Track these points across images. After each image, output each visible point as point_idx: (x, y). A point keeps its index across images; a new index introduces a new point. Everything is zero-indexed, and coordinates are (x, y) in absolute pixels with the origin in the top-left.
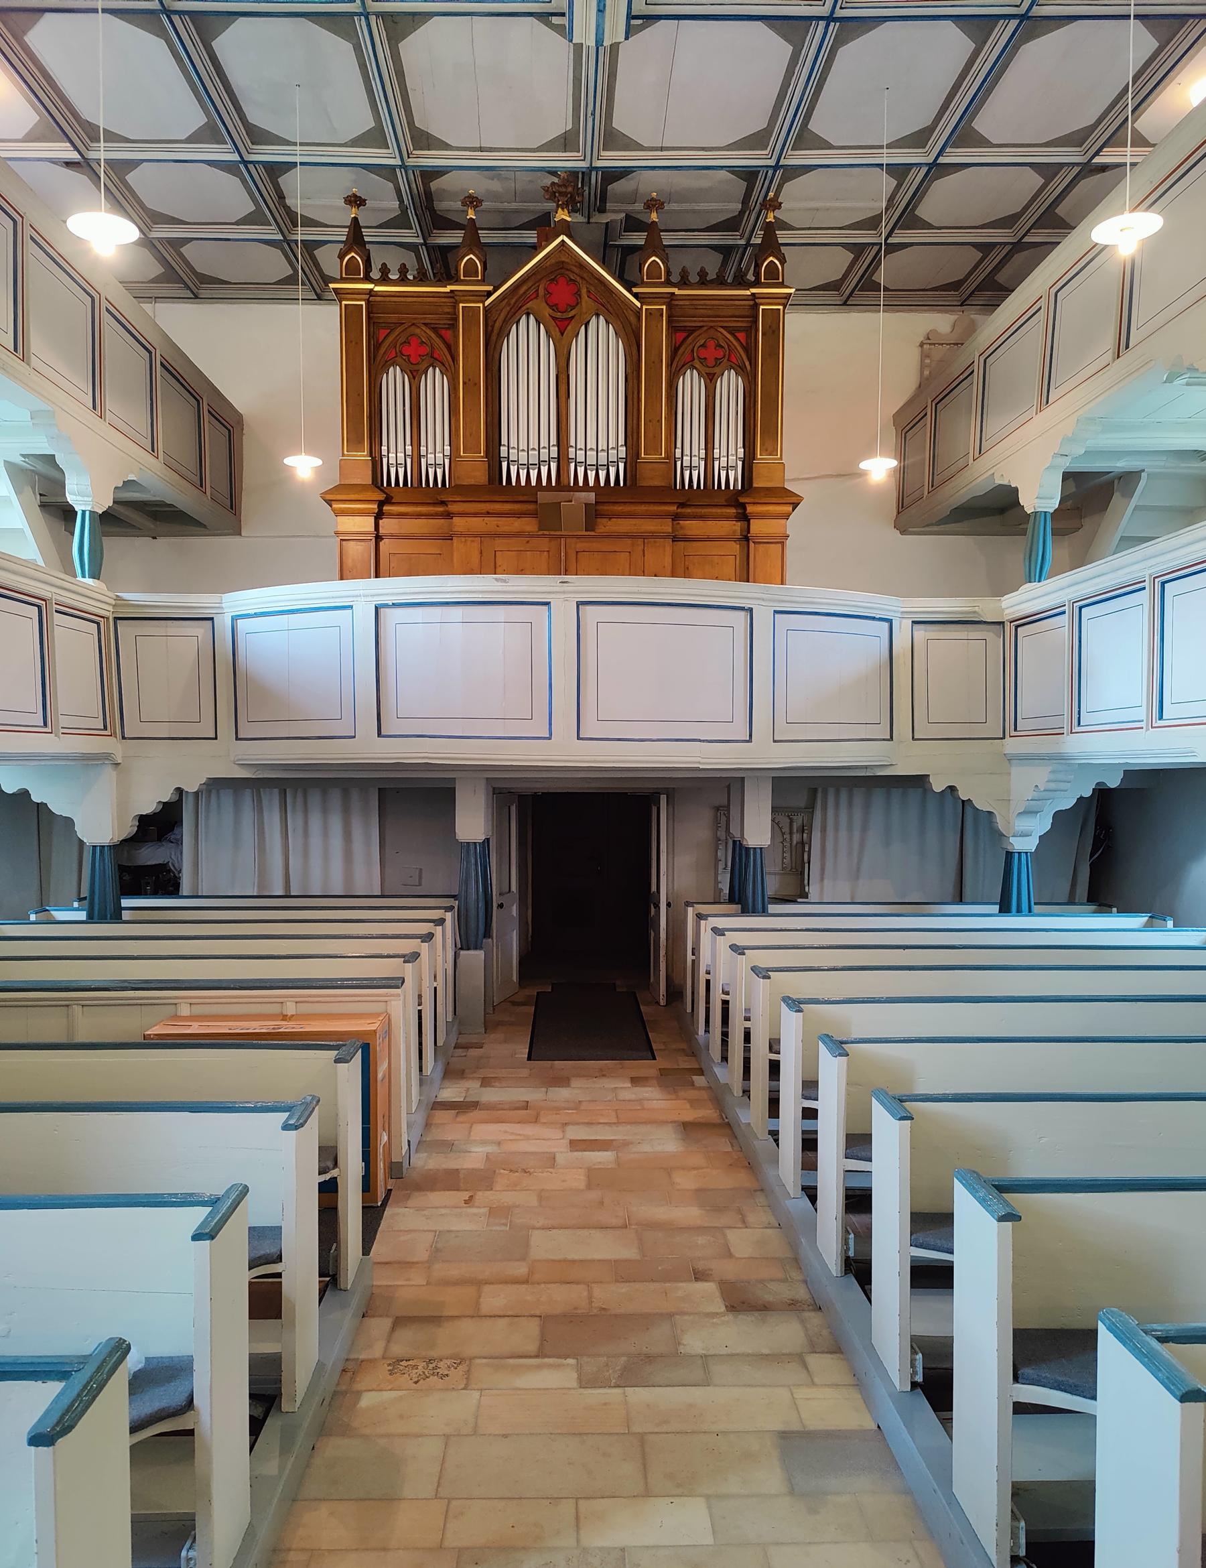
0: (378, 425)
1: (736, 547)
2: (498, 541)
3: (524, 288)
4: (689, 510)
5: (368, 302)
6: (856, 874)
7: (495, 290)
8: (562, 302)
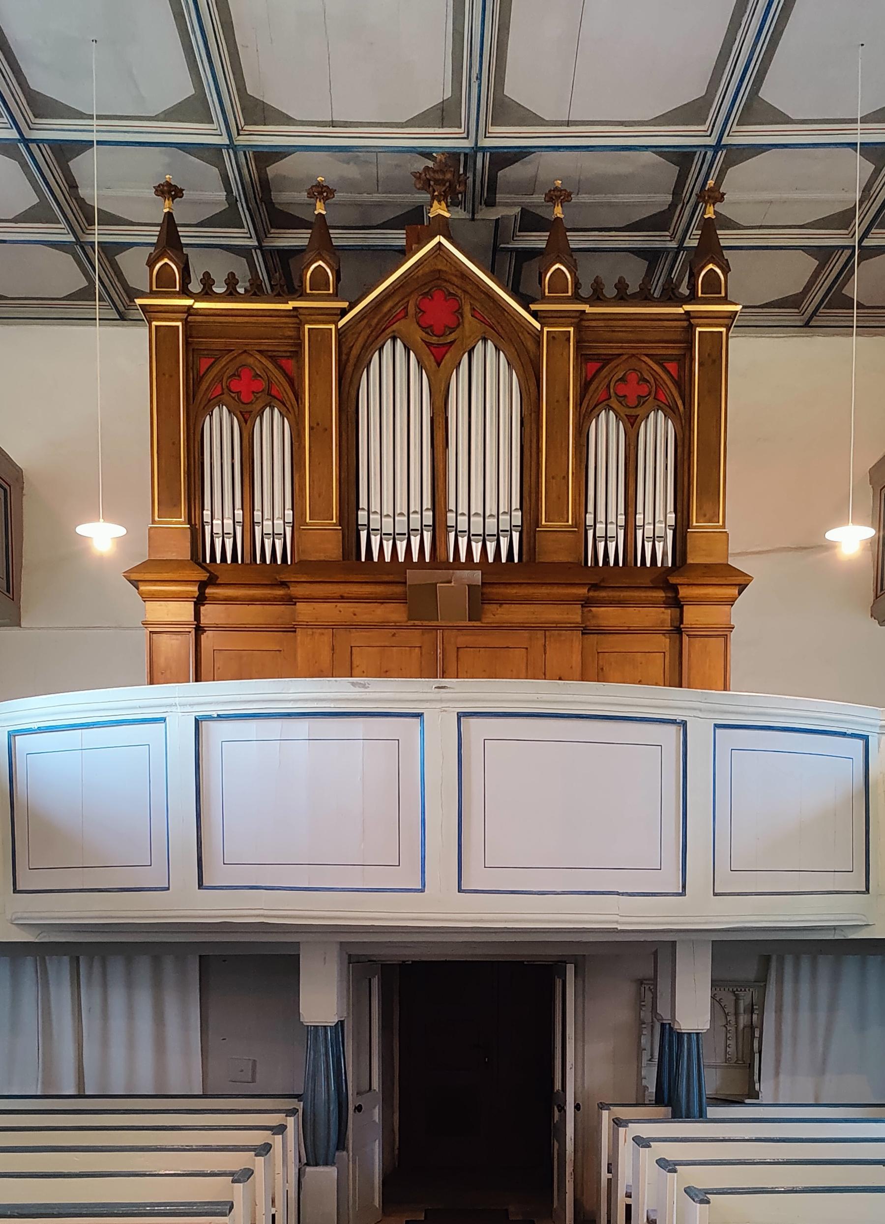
0: (198, 482)
4: (603, 594)
7: (352, 306)
8: (439, 323)
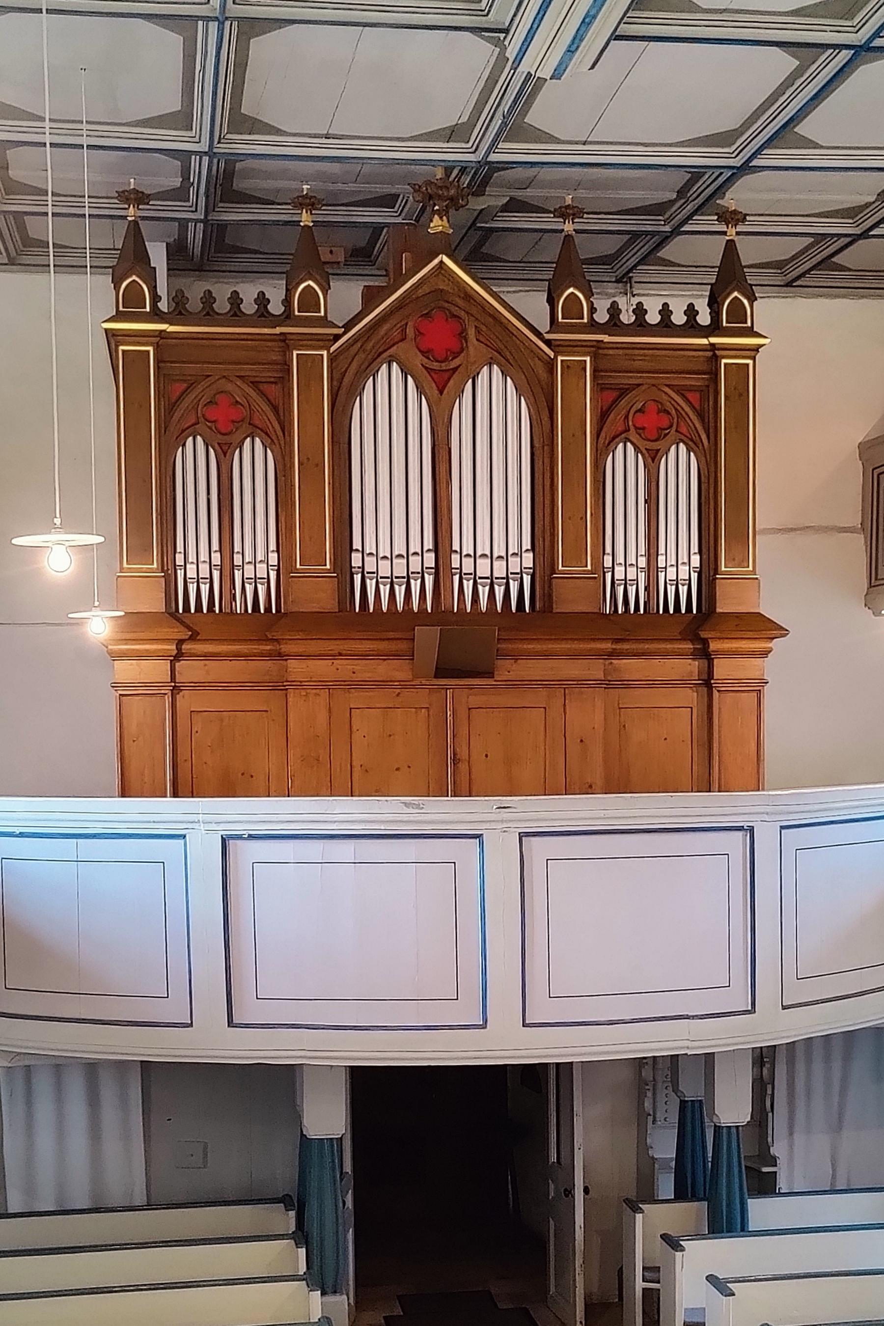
1: (691, 697)
2: (354, 694)
3: (386, 327)
4: (626, 646)
5: (157, 347)
6: (837, 1126)
8: (443, 347)
